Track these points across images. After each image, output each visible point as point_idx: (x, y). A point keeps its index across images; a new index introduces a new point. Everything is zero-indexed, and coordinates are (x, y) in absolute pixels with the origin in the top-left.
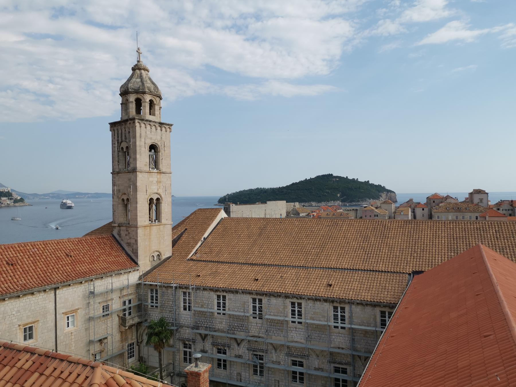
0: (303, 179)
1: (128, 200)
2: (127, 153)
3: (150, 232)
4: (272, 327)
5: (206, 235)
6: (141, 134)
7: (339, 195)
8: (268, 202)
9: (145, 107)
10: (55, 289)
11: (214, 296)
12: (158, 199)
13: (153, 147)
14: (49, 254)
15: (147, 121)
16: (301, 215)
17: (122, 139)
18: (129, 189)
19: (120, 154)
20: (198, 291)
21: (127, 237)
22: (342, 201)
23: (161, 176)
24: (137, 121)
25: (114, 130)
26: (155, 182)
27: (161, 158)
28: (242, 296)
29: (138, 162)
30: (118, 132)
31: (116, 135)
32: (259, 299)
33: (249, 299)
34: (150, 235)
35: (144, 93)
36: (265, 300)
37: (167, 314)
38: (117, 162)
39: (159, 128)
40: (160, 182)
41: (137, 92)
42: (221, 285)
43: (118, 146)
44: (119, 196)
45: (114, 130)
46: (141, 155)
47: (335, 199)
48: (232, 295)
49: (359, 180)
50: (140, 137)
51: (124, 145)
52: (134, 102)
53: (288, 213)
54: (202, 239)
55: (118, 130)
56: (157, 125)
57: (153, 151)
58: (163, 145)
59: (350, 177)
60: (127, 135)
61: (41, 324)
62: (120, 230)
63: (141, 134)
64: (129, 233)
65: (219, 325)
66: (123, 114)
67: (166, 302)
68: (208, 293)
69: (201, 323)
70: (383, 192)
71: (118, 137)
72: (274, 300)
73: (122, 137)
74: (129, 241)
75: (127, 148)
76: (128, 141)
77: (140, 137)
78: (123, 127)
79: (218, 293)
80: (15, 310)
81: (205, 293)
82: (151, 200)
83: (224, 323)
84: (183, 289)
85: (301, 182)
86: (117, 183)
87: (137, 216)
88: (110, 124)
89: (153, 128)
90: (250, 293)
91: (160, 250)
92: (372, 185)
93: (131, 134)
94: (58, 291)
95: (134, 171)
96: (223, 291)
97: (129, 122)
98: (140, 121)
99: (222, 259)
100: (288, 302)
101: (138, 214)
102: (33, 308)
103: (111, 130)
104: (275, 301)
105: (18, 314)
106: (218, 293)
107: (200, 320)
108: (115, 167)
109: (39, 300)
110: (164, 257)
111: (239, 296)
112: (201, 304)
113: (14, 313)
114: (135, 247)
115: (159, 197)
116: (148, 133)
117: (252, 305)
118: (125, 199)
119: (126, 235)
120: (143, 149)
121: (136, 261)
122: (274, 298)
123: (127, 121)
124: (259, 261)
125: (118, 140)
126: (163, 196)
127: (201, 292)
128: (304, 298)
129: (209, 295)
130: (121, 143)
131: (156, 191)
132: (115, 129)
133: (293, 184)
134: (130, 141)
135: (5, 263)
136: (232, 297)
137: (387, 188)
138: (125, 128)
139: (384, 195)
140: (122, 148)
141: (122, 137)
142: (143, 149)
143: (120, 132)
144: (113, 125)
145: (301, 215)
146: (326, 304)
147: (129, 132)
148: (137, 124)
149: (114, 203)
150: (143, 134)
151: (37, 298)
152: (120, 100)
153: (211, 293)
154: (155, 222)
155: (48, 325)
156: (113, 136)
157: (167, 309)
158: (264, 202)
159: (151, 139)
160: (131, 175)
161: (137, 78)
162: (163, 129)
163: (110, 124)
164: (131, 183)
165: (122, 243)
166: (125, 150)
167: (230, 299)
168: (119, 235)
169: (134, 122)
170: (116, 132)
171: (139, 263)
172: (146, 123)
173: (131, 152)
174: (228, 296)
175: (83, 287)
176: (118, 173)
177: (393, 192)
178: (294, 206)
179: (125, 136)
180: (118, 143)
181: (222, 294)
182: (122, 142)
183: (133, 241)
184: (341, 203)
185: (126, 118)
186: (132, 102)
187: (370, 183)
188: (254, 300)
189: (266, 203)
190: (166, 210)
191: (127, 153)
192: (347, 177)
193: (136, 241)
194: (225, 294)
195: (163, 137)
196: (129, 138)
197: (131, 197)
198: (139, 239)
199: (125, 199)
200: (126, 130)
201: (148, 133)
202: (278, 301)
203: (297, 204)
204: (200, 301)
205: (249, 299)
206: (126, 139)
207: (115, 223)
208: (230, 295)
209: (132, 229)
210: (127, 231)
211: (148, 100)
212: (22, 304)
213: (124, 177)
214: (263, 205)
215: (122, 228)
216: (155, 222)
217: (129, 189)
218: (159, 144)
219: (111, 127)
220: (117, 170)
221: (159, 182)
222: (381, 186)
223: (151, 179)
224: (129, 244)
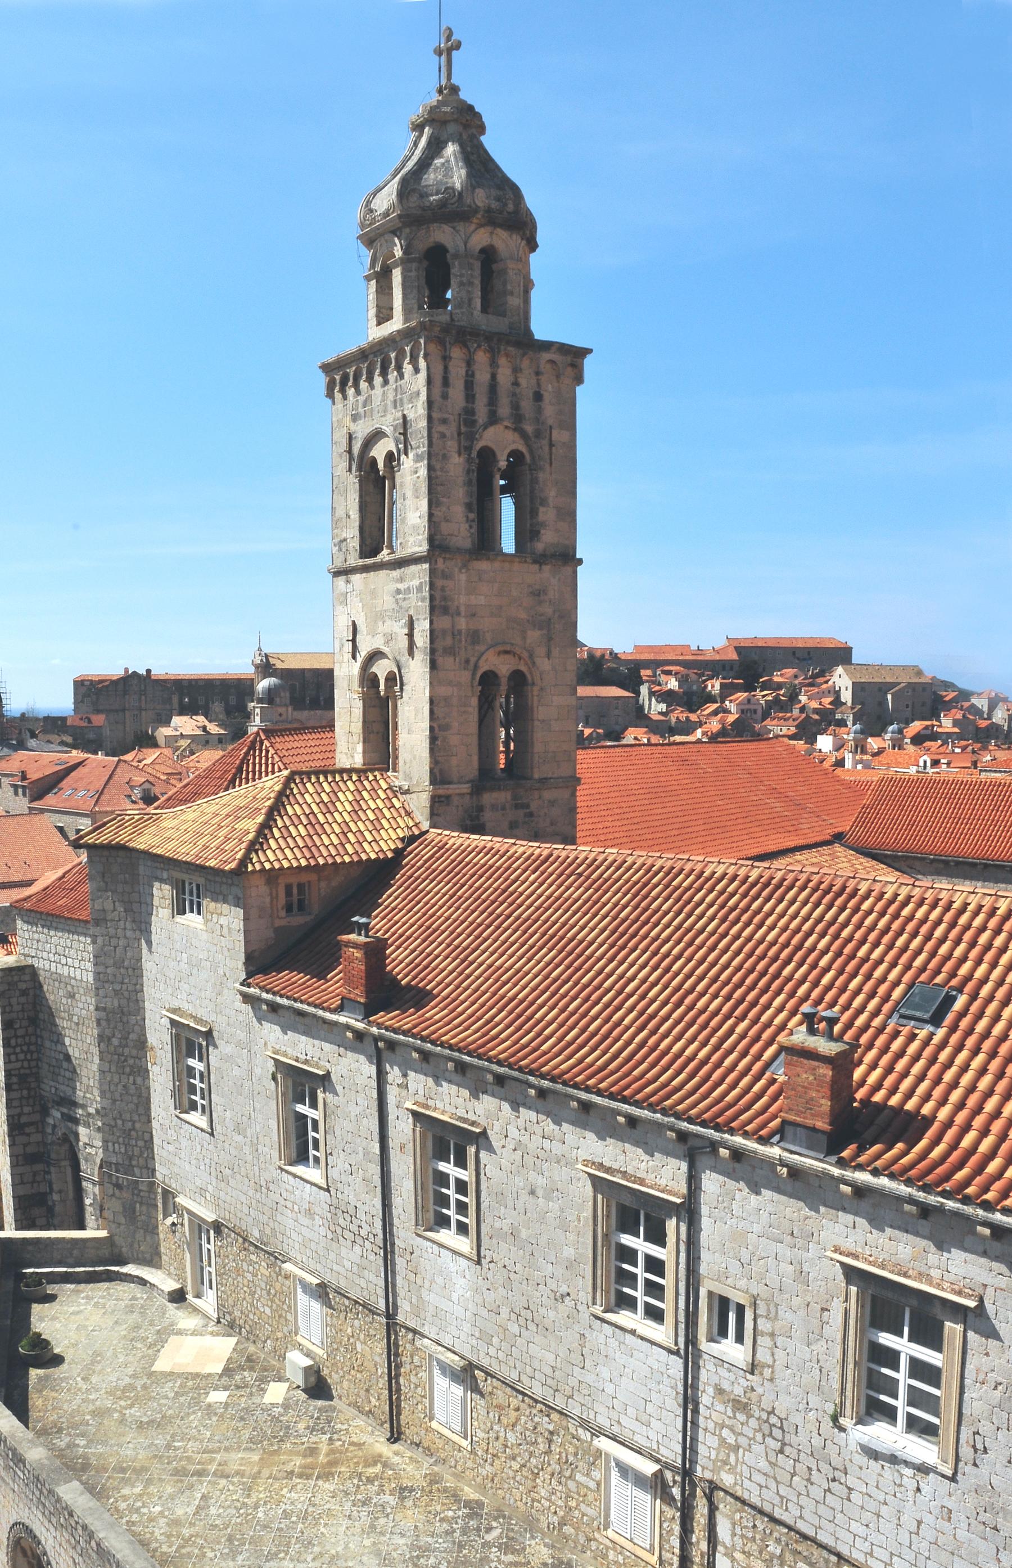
1: (519, 681)
38: (458, 511)
55: (469, 363)
60: (527, 406)
62: (480, 809)
64: (531, 815)
71: (470, 396)
76: (529, 429)
86: (462, 600)
97: (546, 356)
108: (445, 528)
130: (485, 427)
138: (516, 370)
140: (487, 456)
143: (483, 377)
147: (538, 397)
149: (443, 691)
170: (458, 371)
179: (516, 407)
200: (523, 382)
206: (518, 417)
209: (547, 795)
210: (517, 806)
215: (488, 798)
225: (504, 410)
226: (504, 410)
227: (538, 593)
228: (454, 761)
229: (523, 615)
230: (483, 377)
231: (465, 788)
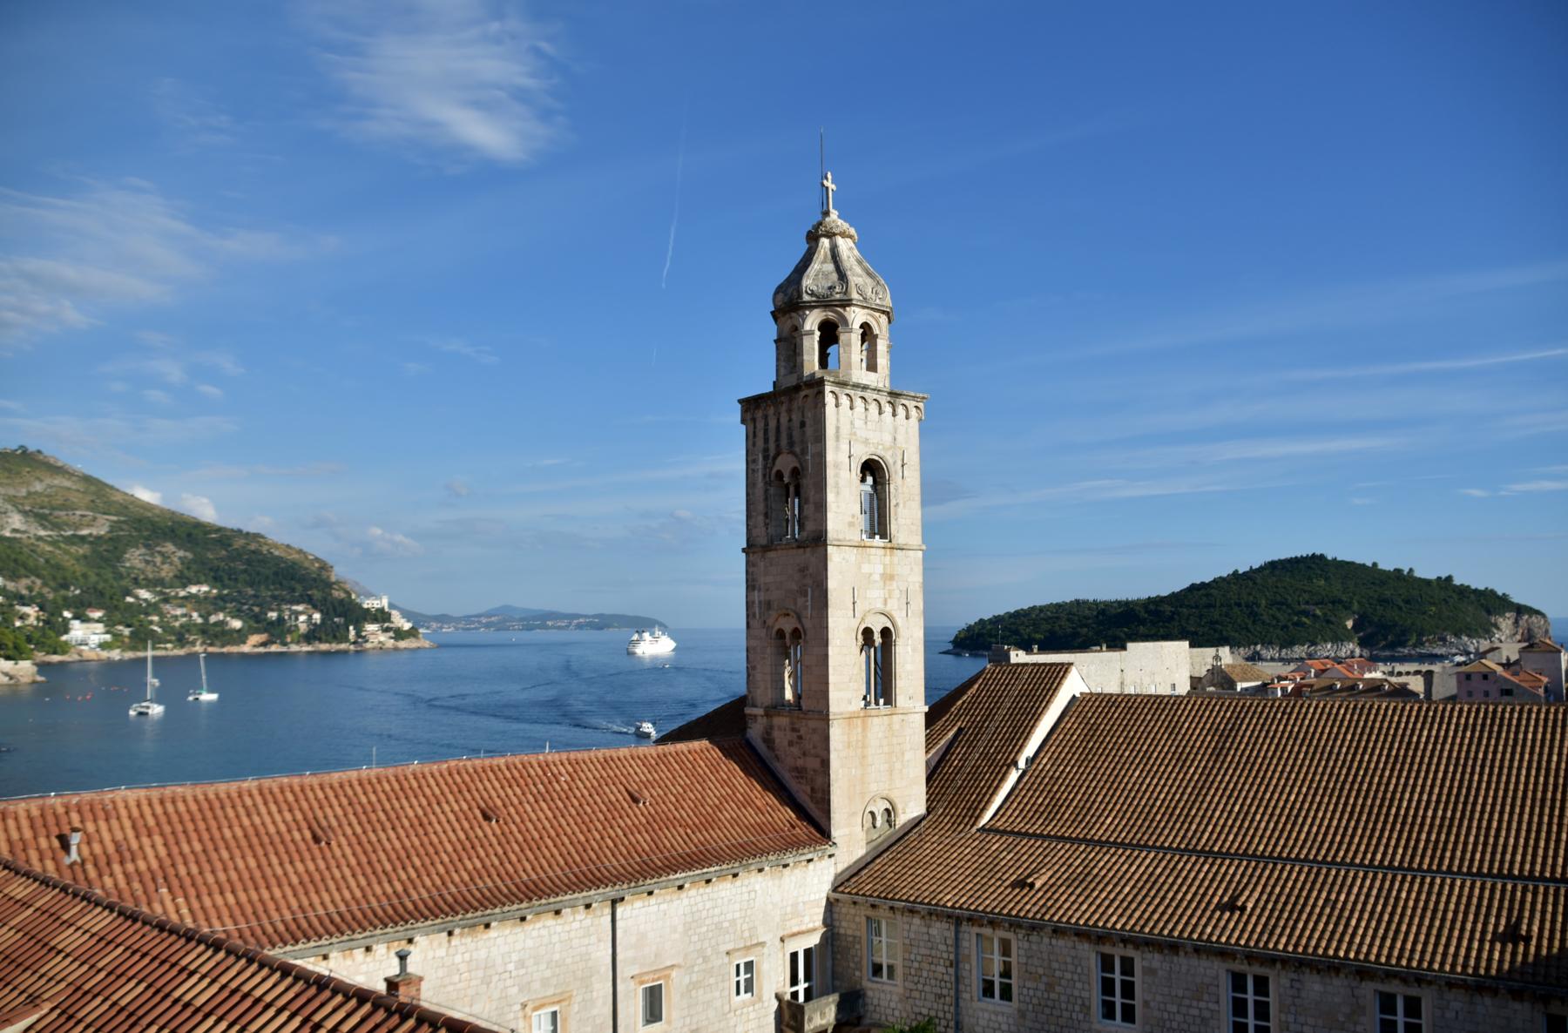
0: (1225, 572)
2: (792, 489)
3: (864, 737)
5: (1030, 749)
6: (838, 428)
7: (1350, 624)
8: (1130, 645)
9: (849, 345)
10: (614, 902)
11: (1090, 956)
12: (886, 633)
13: (872, 468)
14: (586, 793)
15: (856, 386)
16: (1240, 686)
17: (778, 446)
18: (800, 601)
19: (772, 491)
20: (1034, 938)
21: (795, 750)
22: (1363, 643)
23: (896, 559)
24: (828, 388)
25: (754, 420)
26: (877, 577)
27: (893, 502)
28: (1194, 961)
29: (830, 515)
30: (767, 424)
31: (760, 434)
32: (1123, 959)
33: (1217, 972)
34: (864, 747)
35: (847, 303)
36: (1279, 983)
37: (928, 1004)
38: (761, 518)
39: (888, 409)
40: (892, 577)
41: (823, 302)
42: (1116, 922)
43: (765, 467)
44: (770, 622)
45: (754, 420)
46: (838, 493)
47: (1338, 638)
48: (1157, 956)
49: (1418, 574)
50: (837, 438)
51: (785, 463)
52: (818, 333)
53: (1195, 682)
54: (1022, 764)
56: (884, 399)
57: (870, 480)
58: (899, 463)
59: (1387, 565)
60: (796, 434)
61: (576, 1008)
62: (771, 727)
63: (838, 428)
64: (800, 737)
66: (783, 371)
67: (925, 965)
68: (1070, 944)
70: (1502, 614)
71: (766, 440)
72: (1314, 985)
73: (778, 440)
74: (800, 763)
75: (795, 473)
76: (797, 449)
77: (837, 438)
78: (784, 408)
79: (1107, 949)
80: (515, 957)
81: (1060, 943)
82: (867, 633)
84: (981, 926)
85: (1218, 582)
86: (762, 580)
87: (827, 683)
88: (740, 401)
89: (873, 407)
90: (1224, 953)
91: (894, 796)
92: (1464, 591)
93: (809, 430)
94: (620, 909)
95: (818, 540)
96: (1125, 941)
97: (803, 393)
98: (836, 389)
99: (1098, 833)
100: (1368, 991)
101: (832, 679)
102: (557, 957)
103: (743, 421)
104: (1317, 987)
105: (522, 972)
106: (1107, 949)
109: (573, 934)
110: (902, 819)
111: (1182, 962)
112: (1044, 979)
113: (511, 967)
114: (819, 781)
115: (889, 625)
116: (859, 423)
117: (1270, 1000)
118: (788, 629)
119: (791, 744)
120: (844, 474)
121: (822, 822)
122: (1316, 977)
123: (797, 388)
124: (1231, 843)
125: (766, 450)
126: (899, 622)
127: (1046, 940)
128: (1430, 983)
130: (775, 458)
131: (880, 606)
132: (759, 414)
133: (1193, 588)
134: (804, 451)
135: (478, 813)
136: (1156, 964)
137: (1517, 598)
138: (789, 411)
139: (1506, 623)
140: (780, 475)
141: (778, 440)
142: (844, 474)
143: (772, 424)
144: (751, 406)
145: (1240, 686)
146: (1517, 1006)
147: (803, 424)
148: (829, 399)
149: (754, 643)
150: (845, 430)
151: (567, 928)
152: (771, 330)
153: (1079, 946)
154: (877, 703)
155: (595, 1012)
156: (751, 438)
157: (927, 988)
158: (1117, 644)
159: (866, 442)
160: (807, 556)
161: (824, 262)
162: (901, 411)
163: (740, 401)
164: (809, 581)
165: (778, 767)
166: (786, 480)
167: (1150, 971)
168: (768, 740)
169: (821, 393)
170: (760, 425)
171: (836, 833)
172: (852, 392)
173: (807, 482)
174: (1140, 961)
175: (686, 902)
176: (766, 549)
177: (1538, 612)
178: (1217, 658)
179: (790, 436)
180: (766, 458)
181: (1118, 952)
182: (778, 453)
183: (812, 763)
184: (1358, 651)
185: (791, 381)
186: (811, 333)
187: (1457, 581)
188: (1238, 982)
189: (1124, 648)
190: (909, 667)
191: (792, 489)
192: (1375, 564)
193: (826, 764)
194: (1130, 952)
195: (899, 438)
196: (803, 442)
197: (808, 624)
198: (833, 756)
199: (788, 629)
200: (794, 417)
201: (859, 423)
203: (1225, 652)
204: (1041, 971)
205: (1217, 972)
206: (791, 444)
207: (754, 706)
208: (1149, 956)
209: (812, 724)
210: (794, 730)
211: (856, 326)
212: (530, 943)
213: (784, 562)
214: (1115, 655)
215: (777, 721)
216: (877, 703)
217: (800, 601)
218: (889, 457)
219: (744, 412)
220: (763, 541)
221: (888, 577)
222: (1493, 592)
223: (866, 568)
224: (800, 772)
225: (784, 442)
226: (784, 442)
227: (803, 570)
228: (759, 692)
229: (795, 587)
230: (772, 424)
231: (760, 711)
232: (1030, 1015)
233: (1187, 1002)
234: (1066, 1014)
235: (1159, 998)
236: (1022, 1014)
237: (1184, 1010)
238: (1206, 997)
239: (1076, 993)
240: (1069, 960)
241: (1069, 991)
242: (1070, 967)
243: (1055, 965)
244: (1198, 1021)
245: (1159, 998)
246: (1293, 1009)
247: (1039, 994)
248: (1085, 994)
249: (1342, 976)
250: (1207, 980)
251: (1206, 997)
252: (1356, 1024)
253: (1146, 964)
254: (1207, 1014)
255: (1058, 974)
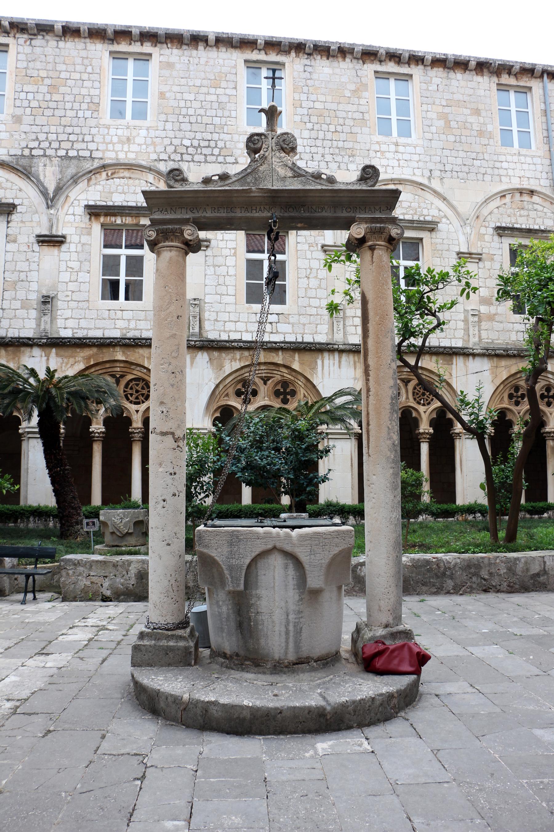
4: (319, 143)
65: (118, 147)
69: (45, 145)
81: (71, 47)
83: (139, 140)
107: (42, 137)
111: (201, 54)
112: (48, 82)
129: (84, 53)
167: (169, 65)
202: (337, 71)
204: (43, 74)
232: (28, 119)
233: (204, 90)
234: (70, 113)
235: (176, 89)
236: (18, 119)
237: (202, 97)
238: (223, 84)
239: (84, 91)
240: (79, 61)
241: (75, 91)
242: (79, 68)
243: (62, 67)
244: (215, 105)
245: (176, 89)
246: (305, 89)
247: (40, 97)
248: (93, 92)
249: (348, 60)
250: (224, 70)
251: (223, 84)
252: (359, 98)
253: (162, 58)
254: (224, 99)
255: (63, 75)
